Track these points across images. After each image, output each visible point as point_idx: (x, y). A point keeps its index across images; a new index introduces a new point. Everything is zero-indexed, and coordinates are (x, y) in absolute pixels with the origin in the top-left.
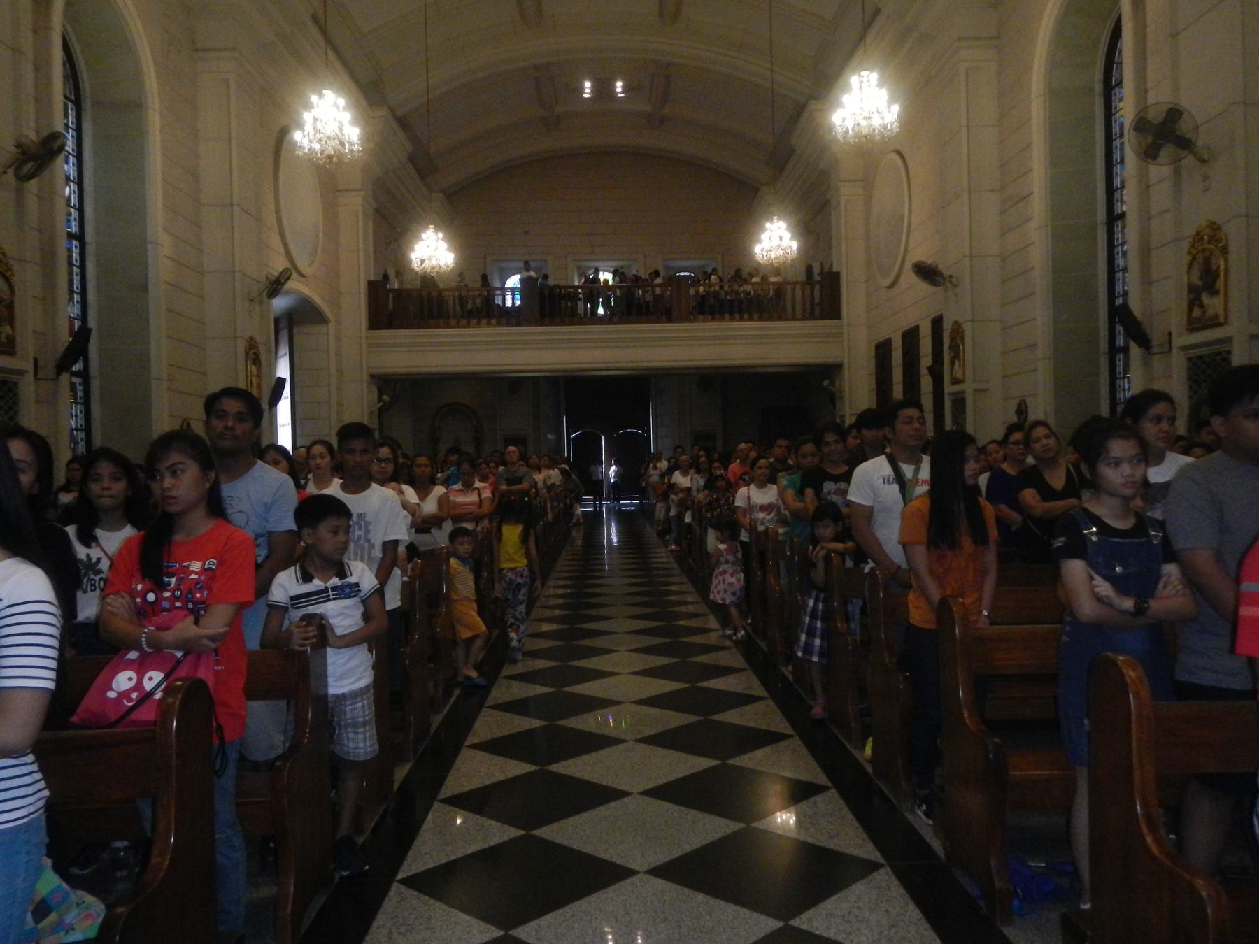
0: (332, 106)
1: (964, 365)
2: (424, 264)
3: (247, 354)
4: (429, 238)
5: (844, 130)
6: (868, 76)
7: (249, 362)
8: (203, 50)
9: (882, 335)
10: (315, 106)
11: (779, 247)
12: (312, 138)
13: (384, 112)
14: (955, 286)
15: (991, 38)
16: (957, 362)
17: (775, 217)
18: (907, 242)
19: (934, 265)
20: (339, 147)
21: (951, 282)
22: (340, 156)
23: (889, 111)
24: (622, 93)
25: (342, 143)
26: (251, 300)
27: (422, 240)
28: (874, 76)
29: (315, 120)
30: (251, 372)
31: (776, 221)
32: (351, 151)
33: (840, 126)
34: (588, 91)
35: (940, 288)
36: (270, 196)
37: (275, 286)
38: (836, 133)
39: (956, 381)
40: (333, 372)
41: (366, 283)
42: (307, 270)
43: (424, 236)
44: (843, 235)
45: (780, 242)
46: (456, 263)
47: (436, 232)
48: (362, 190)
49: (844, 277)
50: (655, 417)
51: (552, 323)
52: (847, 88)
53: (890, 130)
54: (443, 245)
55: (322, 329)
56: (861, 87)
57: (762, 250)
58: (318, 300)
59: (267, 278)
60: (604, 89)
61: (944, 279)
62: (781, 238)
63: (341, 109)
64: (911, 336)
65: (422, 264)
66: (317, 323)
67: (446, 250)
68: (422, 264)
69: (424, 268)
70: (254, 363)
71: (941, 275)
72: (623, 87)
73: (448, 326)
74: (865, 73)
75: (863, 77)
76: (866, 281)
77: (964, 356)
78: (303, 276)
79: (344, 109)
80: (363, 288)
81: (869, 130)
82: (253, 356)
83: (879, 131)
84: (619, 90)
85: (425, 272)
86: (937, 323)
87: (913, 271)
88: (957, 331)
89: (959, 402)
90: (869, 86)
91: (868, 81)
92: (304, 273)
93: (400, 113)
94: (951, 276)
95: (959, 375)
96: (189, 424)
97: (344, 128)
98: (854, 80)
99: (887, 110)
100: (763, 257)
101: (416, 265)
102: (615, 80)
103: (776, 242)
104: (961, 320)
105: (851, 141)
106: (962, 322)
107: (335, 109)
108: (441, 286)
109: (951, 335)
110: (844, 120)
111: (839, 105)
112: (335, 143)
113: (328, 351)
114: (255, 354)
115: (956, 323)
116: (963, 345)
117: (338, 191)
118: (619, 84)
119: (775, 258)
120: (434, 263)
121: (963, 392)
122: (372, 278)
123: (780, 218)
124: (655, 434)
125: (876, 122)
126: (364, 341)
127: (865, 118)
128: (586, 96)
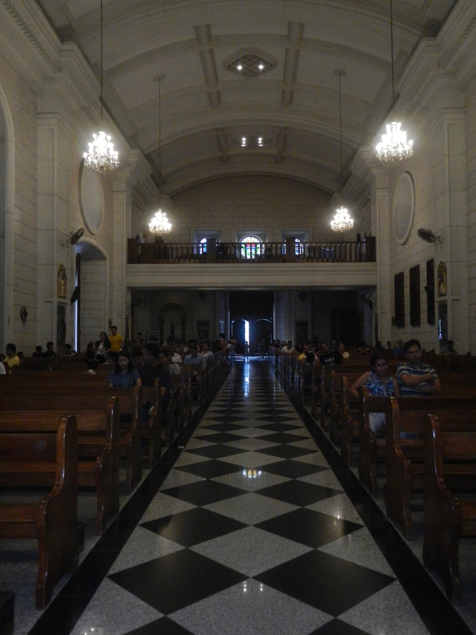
0: (104, 140)
1: (446, 285)
2: (156, 229)
3: (59, 273)
4: (158, 216)
5: (382, 154)
6: (396, 125)
7: (60, 279)
8: (41, 113)
10: (95, 139)
11: (344, 222)
12: (93, 156)
13: (137, 151)
14: (441, 242)
15: (461, 108)
16: (442, 284)
17: (342, 207)
18: (413, 220)
19: (430, 230)
20: (107, 162)
21: (439, 240)
22: (107, 166)
23: (408, 144)
24: (261, 144)
25: (109, 160)
26: (62, 245)
27: (155, 216)
28: (399, 124)
29: (95, 147)
30: (61, 283)
31: (342, 208)
32: (114, 164)
33: (381, 152)
34: (244, 143)
35: (433, 244)
36: (77, 193)
37: (75, 238)
38: (378, 156)
39: (441, 295)
40: (108, 285)
42: (96, 232)
43: (156, 214)
45: (344, 220)
48: (126, 191)
49: (377, 240)
51: (222, 262)
52: (385, 132)
53: (408, 154)
54: (166, 220)
55: (103, 262)
56: (392, 130)
57: (335, 224)
58: (100, 247)
59: (71, 234)
60: (252, 142)
61: (435, 238)
62: (345, 218)
63: (109, 141)
64: (415, 271)
65: (154, 229)
66: (101, 259)
67: (168, 222)
68: (154, 229)
69: (156, 231)
70: (63, 278)
71: (434, 237)
72: (262, 141)
73: (168, 263)
74: (394, 123)
75: (393, 125)
76: (389, 242)
77: (446, 280)
78: (92, 234)
79: (111, 141)
80: (125, 242)
81: (396, 153)
82: (62, 274)
83: (402, 154)
84: (260, 142)
85: (156, 234)
86: (430, 264)
87: (418, 234)
88: (442, 267)
89: (443, 307)
90: (396, 130)
91: (396, 127)
92: (94, 233)
93: (146, 152)
94: (439, 237)
95: (443, 291)
96: (25, 310)
97: (110, 152)
98: (388, 126)
99: (407, 143)
100: (335, 228)
101: (151, 229)
102: (258, 137)
103: (342, 220)
104: (445, 261)
105: (386, 161)
106: (445, 262)
107: (105, 141)
108: (166, 242)
109: (438, 269)
110: (382, 149)
111: (380, 140)
112: (104, 160)
113: (105, 274)
114: (63, 273)
115: (441, 262)
116: (446, 275)
117: (113, 192)
118: (260, 139)
119: (342, 228)
120: (161, 229)
121: (446, 301)
122: (130, 237)
123: (344, 207)
125: (400, 150)
126: (124, 268)
127: (394, 148)
128: (243, 145)
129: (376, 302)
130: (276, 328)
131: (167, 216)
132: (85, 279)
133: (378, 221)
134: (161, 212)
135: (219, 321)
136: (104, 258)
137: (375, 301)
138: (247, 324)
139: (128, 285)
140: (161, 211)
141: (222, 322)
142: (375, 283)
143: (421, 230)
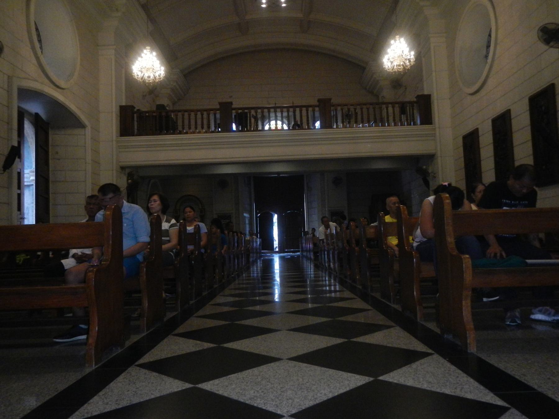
9: (468, 128)
17: (397, 37)
27: (142, 57)
41: (118, 108)
42: (62, 84)
44: (434, 69)
46: (165, 71)
47: (151, 53)
50: (307, 203)
58: (73, 107)
76: (450, 99)
78: (58, 87)
92: (57, 84)
103: (399, 52)
113: (85, 146)
117: (98, 46)
122: (124, 104)
123: (401, 37)
124: (308, 212)
126: (114, 143)
128: (264, 6)
129: (435, 175)
130: (307, 219)
131: (158, 56)
132: (57, 153)
133: (434, 74)
134: (149, 52)
135: (243, 214)
136: (82, 126)
137: (434, 174)
138: (275, 218)
139: (120, 164)
140: (149, 49)
141: (246, 215)
142: (433, 152)
143: (546, 26)
